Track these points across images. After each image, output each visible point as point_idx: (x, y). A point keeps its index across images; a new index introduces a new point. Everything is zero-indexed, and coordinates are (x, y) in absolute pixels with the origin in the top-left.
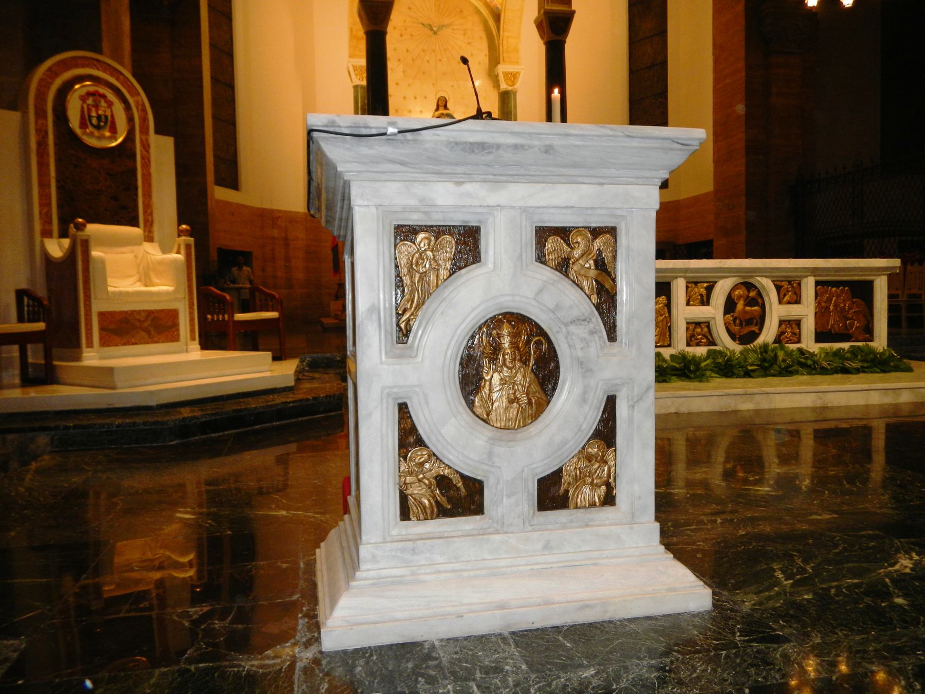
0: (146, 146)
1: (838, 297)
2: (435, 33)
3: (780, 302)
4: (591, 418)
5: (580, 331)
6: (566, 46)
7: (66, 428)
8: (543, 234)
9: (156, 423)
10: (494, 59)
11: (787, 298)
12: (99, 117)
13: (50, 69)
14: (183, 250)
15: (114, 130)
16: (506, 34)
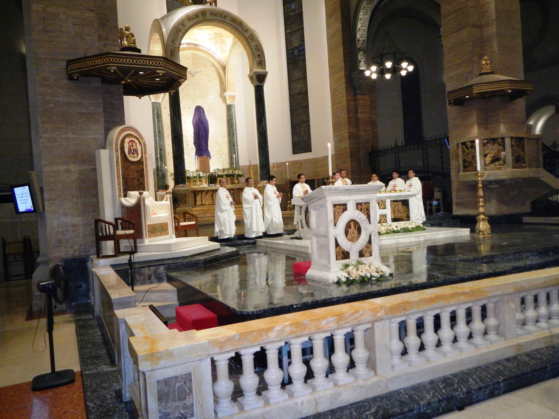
0: (146, 159)
1: (398, 205)
2: (193, 76)
3: (379, 209)
4: (367, 239)
5: (365, 222)
6: (265, 88)
7: (170, 264)
8: (357, 204)
9: (198, 260)
10: (223, 89)
11: (381, 207)
12: (133, 150)
13: (118, 133)
14: (169, 199)
15: (138, 154)
16: (229, 77)
